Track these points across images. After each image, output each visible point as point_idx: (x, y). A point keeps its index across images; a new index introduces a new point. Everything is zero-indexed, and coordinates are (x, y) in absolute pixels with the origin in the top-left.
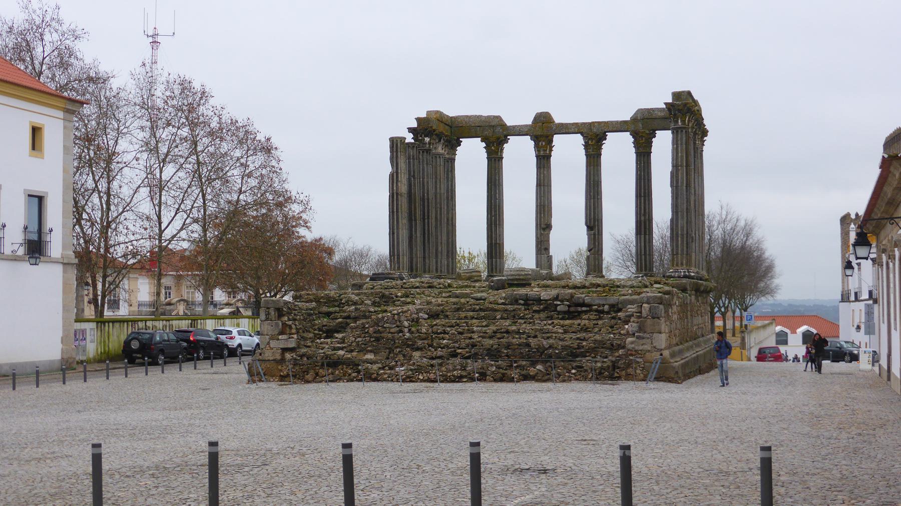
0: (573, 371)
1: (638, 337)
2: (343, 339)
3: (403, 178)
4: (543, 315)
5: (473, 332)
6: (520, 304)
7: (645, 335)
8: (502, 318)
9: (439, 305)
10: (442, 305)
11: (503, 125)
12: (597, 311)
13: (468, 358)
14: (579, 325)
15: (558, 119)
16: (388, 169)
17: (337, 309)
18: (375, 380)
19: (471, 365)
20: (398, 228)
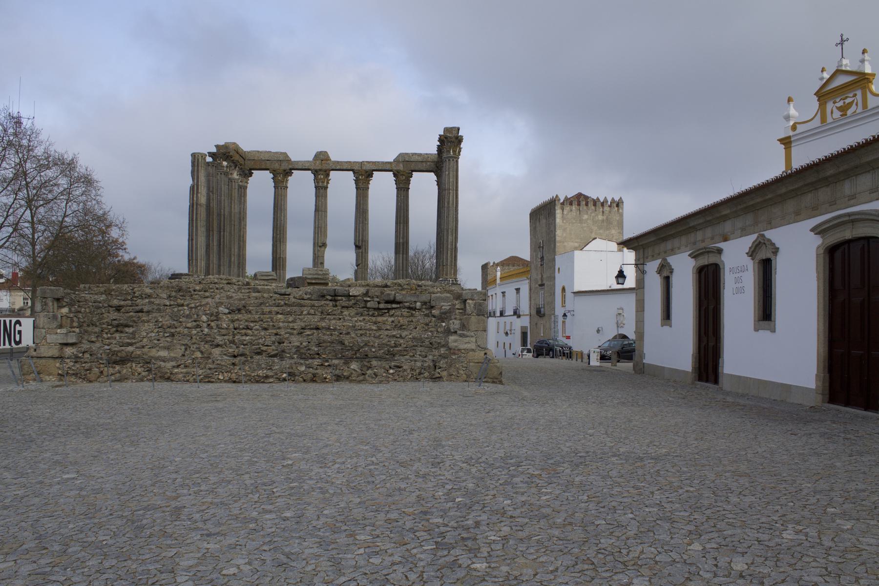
0: (391, 371)
1: (461, 336)
2: (133, 333)
3: (203, 191)
4: (353, 311)
5: (279, 328)
6: (327, 300)
7: (468, 333)
8: (309, 314)
9: (240, 300)
10: (244, 299)
11: (289, 161)
12: (409, 308)
13: (275, 356)
14: (393, 322)
15: (334, 157)
16: (190, 182)
17: (129, 302)
18: (169, 379)
20: (196, 235)
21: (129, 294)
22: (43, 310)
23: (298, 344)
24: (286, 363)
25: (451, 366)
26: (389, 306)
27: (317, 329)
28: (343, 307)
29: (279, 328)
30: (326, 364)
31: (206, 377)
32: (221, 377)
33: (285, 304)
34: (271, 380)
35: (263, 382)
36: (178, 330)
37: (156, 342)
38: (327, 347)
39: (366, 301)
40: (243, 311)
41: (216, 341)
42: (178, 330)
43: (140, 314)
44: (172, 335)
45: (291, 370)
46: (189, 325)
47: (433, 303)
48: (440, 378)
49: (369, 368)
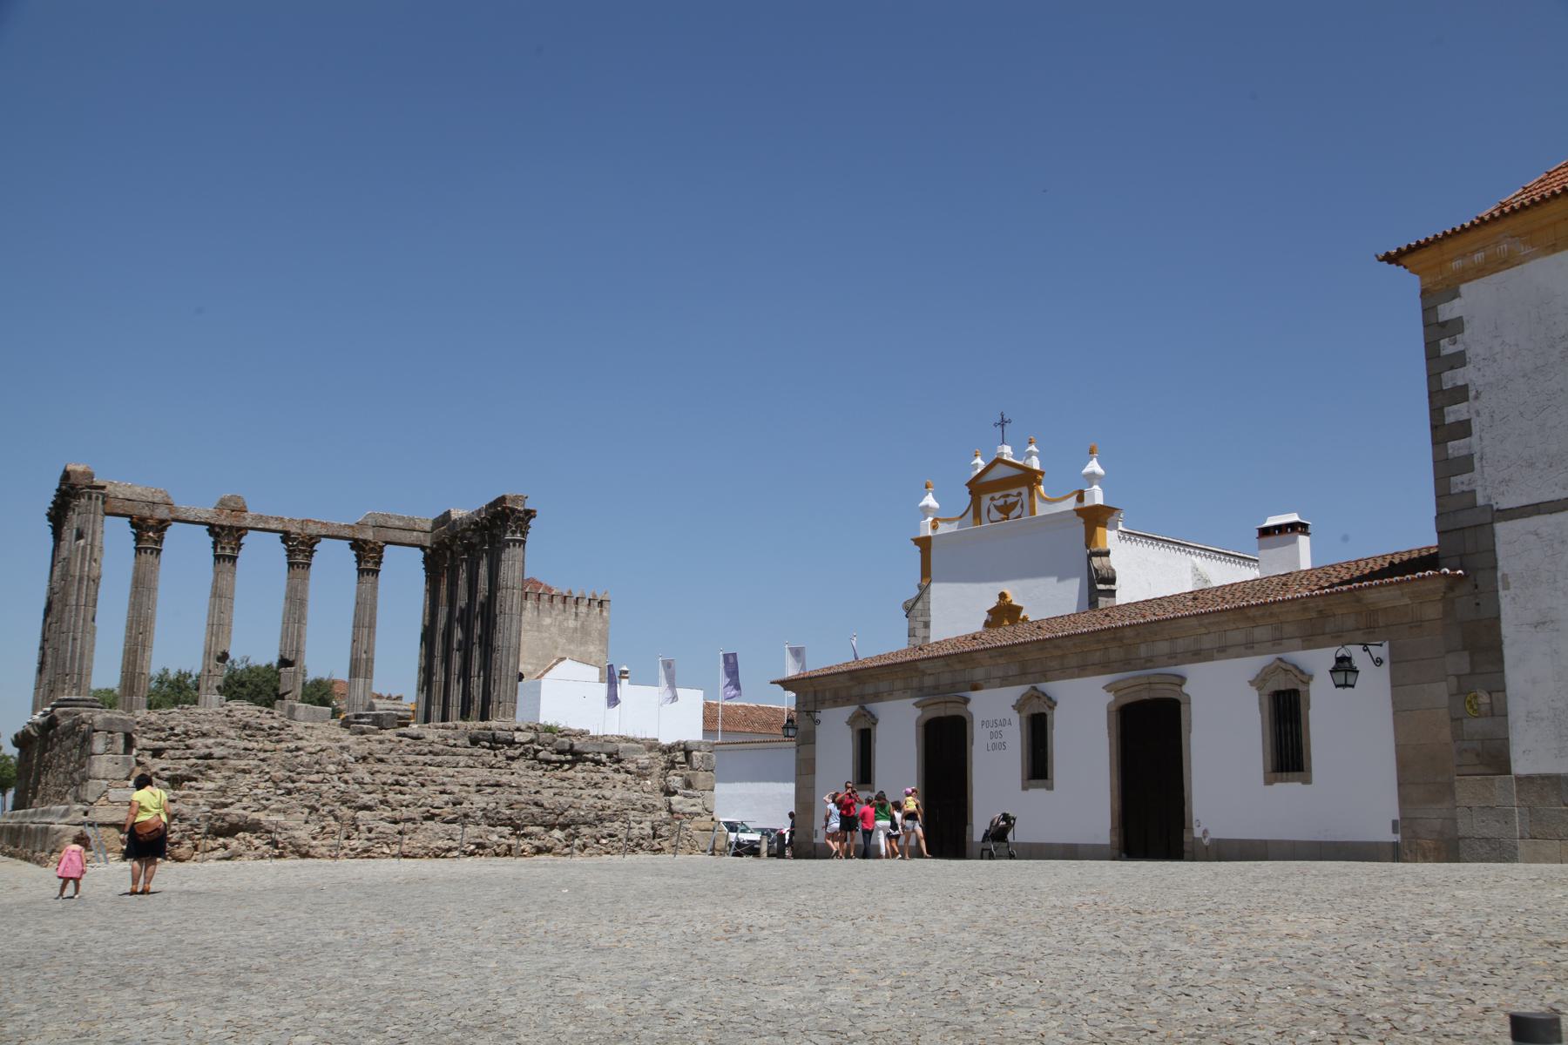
2: (223, 791)
12: (592, 760)
18: (306, 855)
21: (163, 730)
22: (107, 751)
24: (472, 830)
26: (562, 758)
27: (498, 785)
28: (509, 758)
31: (366, 850)
34: (456, 853)
39: (537, 751)
40: (371, 760)
41: (360, 802)
44: (289, 792)
46: (314, 777)
47: (622, 756)
48: (661, 850)
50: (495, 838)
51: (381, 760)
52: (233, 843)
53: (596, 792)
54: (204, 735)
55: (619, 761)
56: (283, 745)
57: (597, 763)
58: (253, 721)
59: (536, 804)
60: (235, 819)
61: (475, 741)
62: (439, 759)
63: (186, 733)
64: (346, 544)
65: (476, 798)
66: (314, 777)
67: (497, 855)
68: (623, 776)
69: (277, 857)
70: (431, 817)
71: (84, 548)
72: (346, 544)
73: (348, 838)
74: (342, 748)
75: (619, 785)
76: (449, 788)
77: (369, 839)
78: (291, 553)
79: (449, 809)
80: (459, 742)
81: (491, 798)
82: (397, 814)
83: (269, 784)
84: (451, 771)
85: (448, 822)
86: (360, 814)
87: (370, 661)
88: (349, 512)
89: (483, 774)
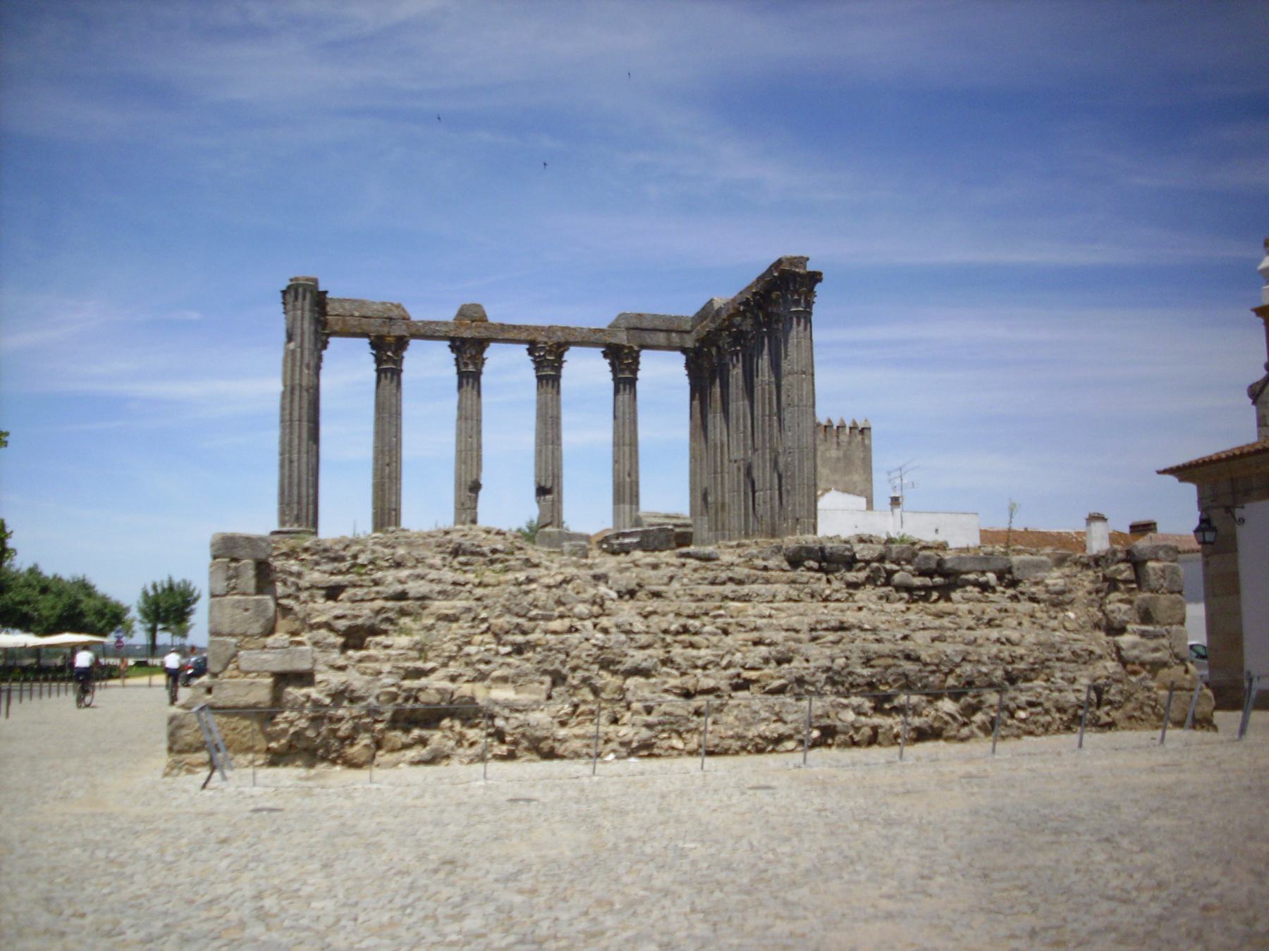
2: (422, 650)
10: (627, 569)
12: (976, 584)
13: (780, 690)
14: (970, 612)
15: (495, 315)
18: (550, 755)
19: (796, 710)
21: (342, 559)
23: (828, 663)
25: (1128, 699)
26: (927, 581)
29: (756, 629)
30: (887, 706)
32: (678, 743)
33: (731, 579)
34: (790, 745)
35: (773, 751)
36: (531, 637)
37: (482, 667)
38: (887, 667)
39: (890, 573)
40: (640, 594)
41: (628, 663)
42: (531, 637)
43: (403, 603)
44: (519, 650)
45: (828, 722)
46: (556, 625)
47: (1017, 574)
48: (1110, 726)
49: (974, 709)
50: (850, 716)
51: (657, 595)
52: (436, 737)
53: (994, 633)
54: (398, 565)
55: (1014, 583)
56: (510, 576)
57: (985, 587)
58: (467, 543)
59: (908, 657)
60: (435, 698)
61: (795, 560)
62: (745, 589)
63: (372, 562)
64: (598, 352)
65: (813, 650)
66: (556, 625)
67: (855, 744)
68: (1025, 606)
69: (502, 758)
70: (744, 685)
71: (293, 352)
72: (598, 352)
73: (615, 721)
74: (597, 578)
75: (1026, 622)
76: (769, 635)
77: (649, 726)
78: (539, 364)
79: (770, 669)
80: (770, 563)
81: (836, 650)
82: (689, 682)
83: (488, 638)
84: (765, 609)
85: (774, 692)
86: (632, 682)
87: (635, 485)
88: (598, 316)
89: (818, 611)
